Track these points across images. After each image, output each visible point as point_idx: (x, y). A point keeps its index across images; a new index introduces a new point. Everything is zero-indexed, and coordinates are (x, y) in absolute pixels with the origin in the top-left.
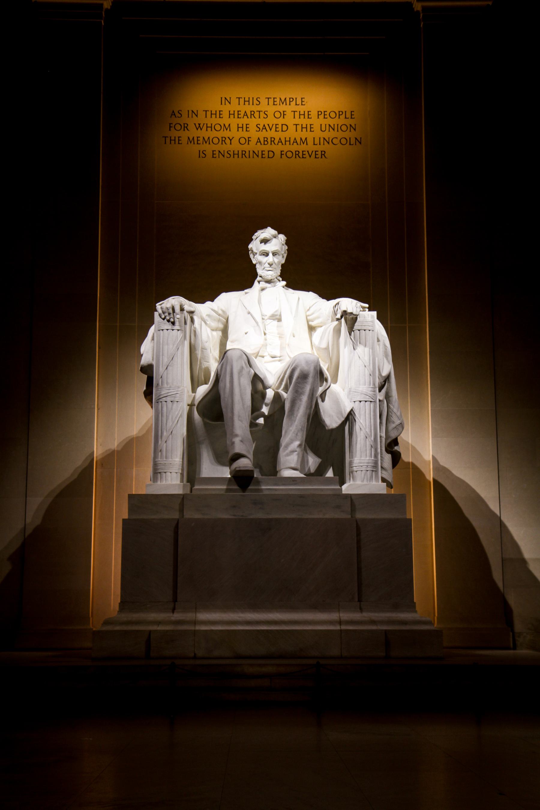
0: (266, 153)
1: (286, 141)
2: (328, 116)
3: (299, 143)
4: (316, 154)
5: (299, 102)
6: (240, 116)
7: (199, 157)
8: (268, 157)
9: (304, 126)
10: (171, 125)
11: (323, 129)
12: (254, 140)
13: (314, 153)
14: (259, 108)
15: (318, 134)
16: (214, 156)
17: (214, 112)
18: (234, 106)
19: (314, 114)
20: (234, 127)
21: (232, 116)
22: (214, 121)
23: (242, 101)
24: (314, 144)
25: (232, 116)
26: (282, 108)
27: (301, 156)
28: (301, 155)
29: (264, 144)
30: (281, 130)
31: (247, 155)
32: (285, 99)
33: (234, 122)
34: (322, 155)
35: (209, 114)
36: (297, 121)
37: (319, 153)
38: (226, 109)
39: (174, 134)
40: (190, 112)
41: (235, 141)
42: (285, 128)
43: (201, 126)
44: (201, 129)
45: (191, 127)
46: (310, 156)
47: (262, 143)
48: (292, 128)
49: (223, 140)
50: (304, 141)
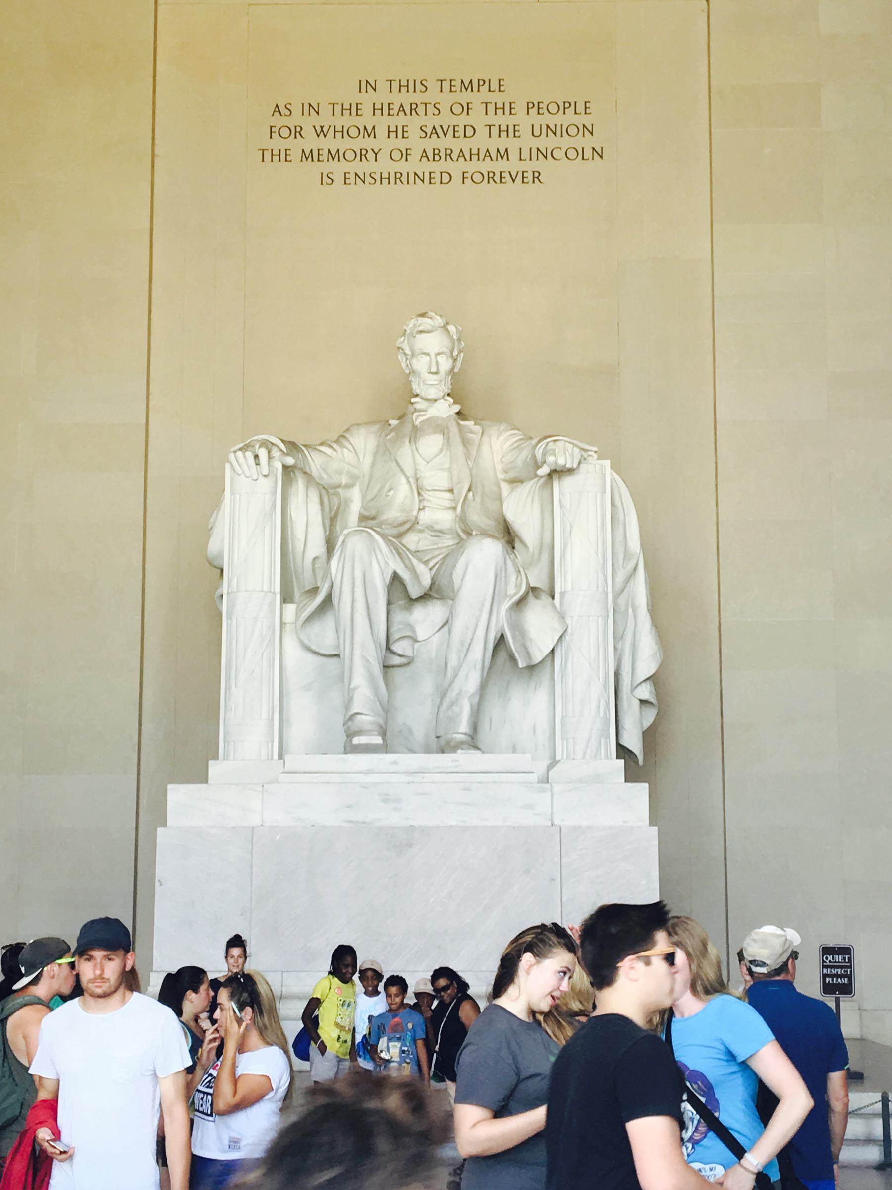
0: (437, 176)
1: (471, 155)
3: (494, 158)
4: (523, 177)
6: (391, 112)
9: (504, 128)
11: (537, 133)
12: (416, 154)
13: (520, 174)
14: (425, 98)
15: (527, 142)
16: (347, 181)
17: (347, 106)
18: (383, 96)
19: (520, 108)
20: (381, 132)
21: (378, 112)
22: (346, 121)
23: (395, 86)
25: (378, 112)
26: (465, 97)
27: (498, 180)
28: (497, 178)
32: (471, 82)
33: (382, 123)
36: (491, 119)
37: (529, 175)
38: (367, 99)
39: (277, 144)
41: (383, 156)
42: (470, 132)
43: (325, 130)
44: (325, 136)
45: (308, 132)
46: (514, 181)
47: (431, 158)
48: (482, 132)
49: (362, 155)
50: (503, 155)
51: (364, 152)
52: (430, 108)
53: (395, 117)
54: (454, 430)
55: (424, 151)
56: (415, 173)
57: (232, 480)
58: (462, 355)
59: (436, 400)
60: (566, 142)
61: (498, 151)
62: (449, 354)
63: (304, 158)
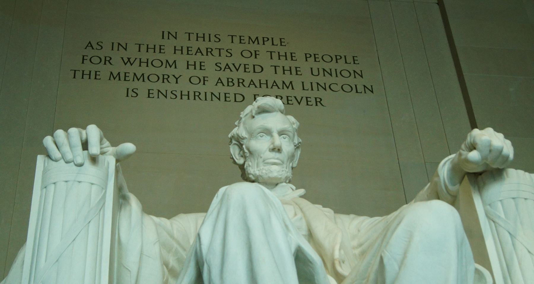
1: (260, 84)
2: (320, 59)
3: (281, 87)
5: (277, 41)
7: (127, 96)
8: (235, 101)
9: (287, 68)
10: (85, 58)
11: (315, 73)
14: (219, 45)
18: (182, 41)
19: (300, 56)
22: (151, 56)
24: (304, 89)
26: (253, 47)
29: (228, 85)
30: (252, 70)
31: (202, 96)
33: (182, 60)
34: (316, 102)
35: (144, 48)
38: (169, 44)
39: (88, 67)
40: (116, 46)
42: (258, 69)
43: (132, 61)
44: (131, 65)
46: (299, 103)
49: (165, 78)
51: (166, 77)
52: (223, 53)
53: (194, 56)
54: (305, 203)
55: (220, 79)
56: (212, 93)
57: (45, 172)
58: (299, 152)
59: (277, 185)
60: (340, 80)
61: (284, 82)
62: (291, 134)
63: (112, 78)
